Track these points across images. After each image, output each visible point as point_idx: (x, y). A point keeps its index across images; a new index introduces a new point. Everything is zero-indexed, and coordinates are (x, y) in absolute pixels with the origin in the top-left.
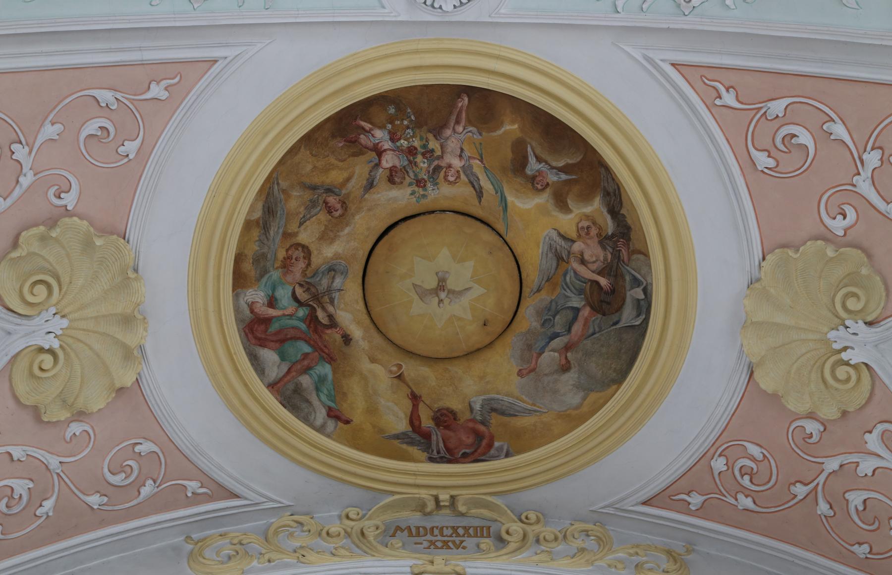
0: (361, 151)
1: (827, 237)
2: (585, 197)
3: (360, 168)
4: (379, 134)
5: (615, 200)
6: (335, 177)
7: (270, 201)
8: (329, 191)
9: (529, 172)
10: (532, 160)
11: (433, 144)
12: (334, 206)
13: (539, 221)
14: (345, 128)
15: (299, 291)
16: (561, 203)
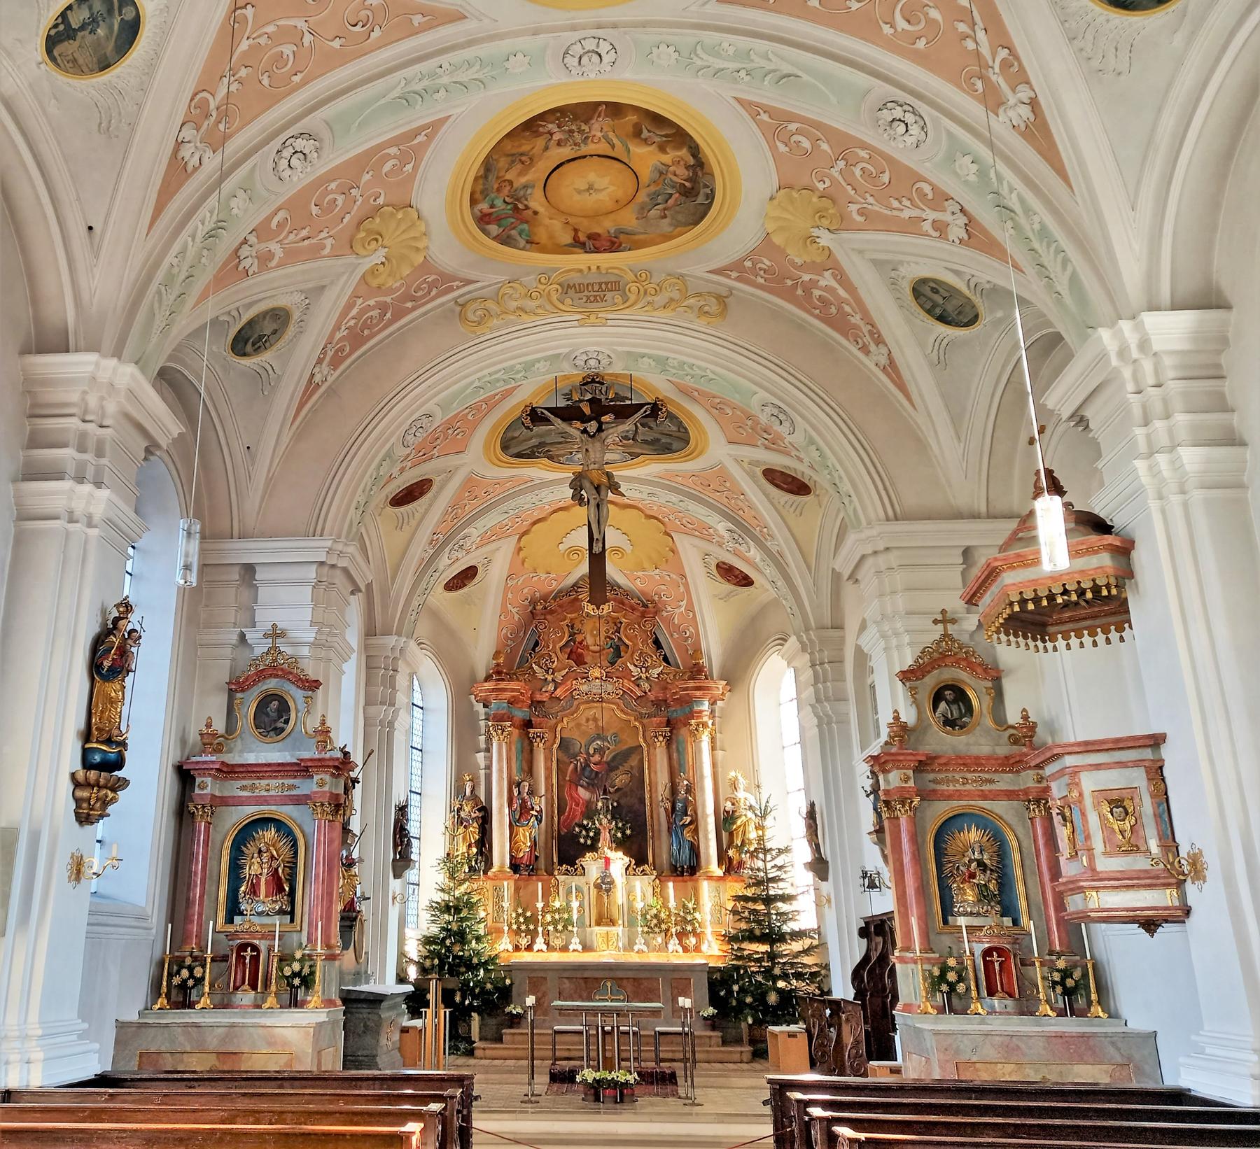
0: (541, 134)
1: (812, 189)
2: (678, 148)
3: (540, 142)
4: (550, 126)
5: (695, 150)
6: (525, 148)
7: (488, 166)
8: (522, 154)
9: (643, 136)
10: (645, 131)
11: (584, 127)
12: (525, 161)
13: (646, 158)
14: (531, 126)
15: (507, 199)
16: (662, 149)
